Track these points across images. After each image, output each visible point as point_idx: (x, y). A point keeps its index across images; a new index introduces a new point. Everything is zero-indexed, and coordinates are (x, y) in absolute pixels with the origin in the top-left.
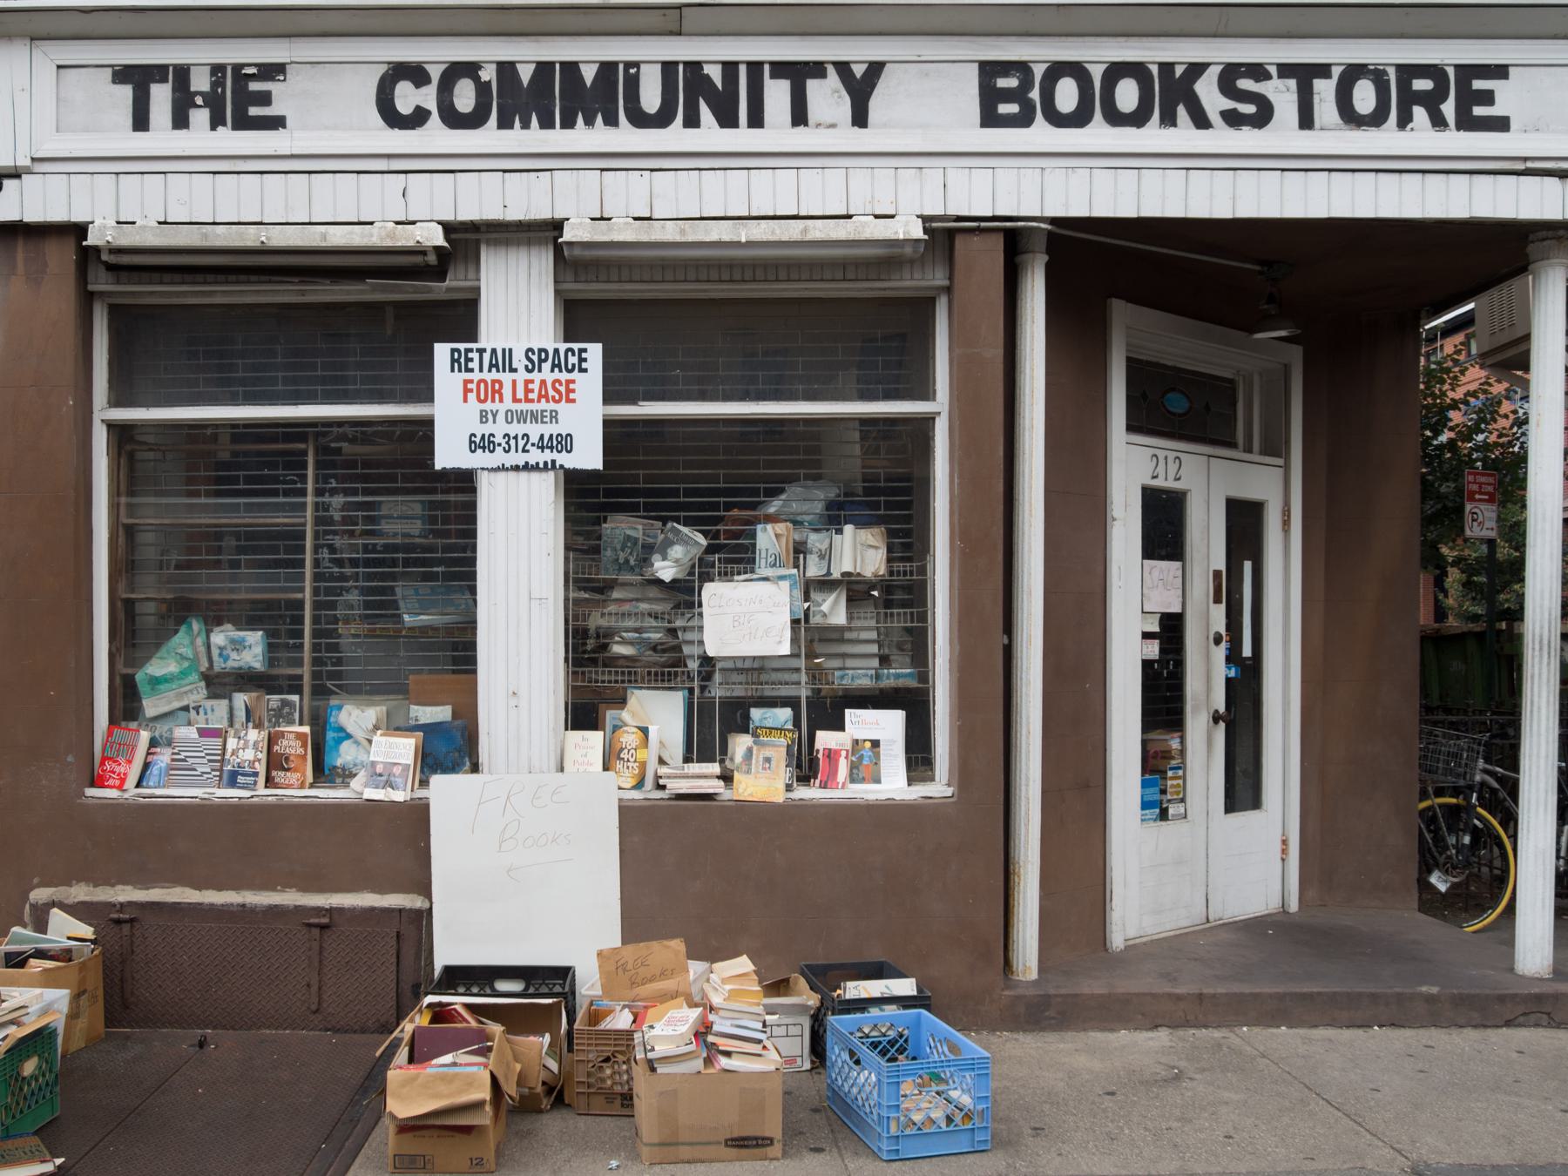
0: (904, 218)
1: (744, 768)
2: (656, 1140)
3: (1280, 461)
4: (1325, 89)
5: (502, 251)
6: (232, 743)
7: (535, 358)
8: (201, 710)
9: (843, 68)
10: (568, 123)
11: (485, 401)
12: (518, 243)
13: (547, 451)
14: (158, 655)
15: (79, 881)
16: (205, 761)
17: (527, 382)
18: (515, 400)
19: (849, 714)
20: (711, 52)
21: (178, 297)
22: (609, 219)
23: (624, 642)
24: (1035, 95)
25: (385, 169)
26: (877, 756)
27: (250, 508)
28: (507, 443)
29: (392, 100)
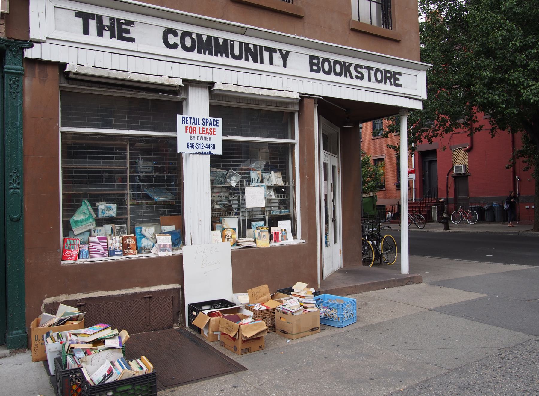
0: (295, 93)
1: (259, 238)
2: (296, 333)
4: (372, 73)
5: (194, 89)
6: (110, 242)
7: (205, 121)
8: (96, 231)
9: (281, 51)
10: (216, 55)
11: (191, 133)
12: (199, 87)
13: (208, 149)
14: (77, 213)
15: (62, 294)
16: (102, 248)
17: (203, 128)
18: (200, 133)
19: (279, 222)
20: (252, 41)
21: (88, 91)
22: (227, 84)
23: (217, 204)
24: (320, 65)
25: (166, 60)
26: (286, 233)
27: (103, 163)
28: (198, 146)
29: (167, 39)
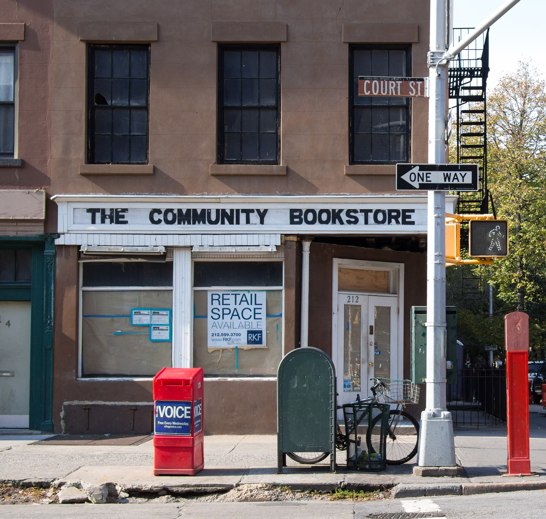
3: (397, 295)
4: (371, 215)
9: (258, 211)
10: (194, 223)
15: (75, 400)
24: (303, 217)
25: (151, 233)
